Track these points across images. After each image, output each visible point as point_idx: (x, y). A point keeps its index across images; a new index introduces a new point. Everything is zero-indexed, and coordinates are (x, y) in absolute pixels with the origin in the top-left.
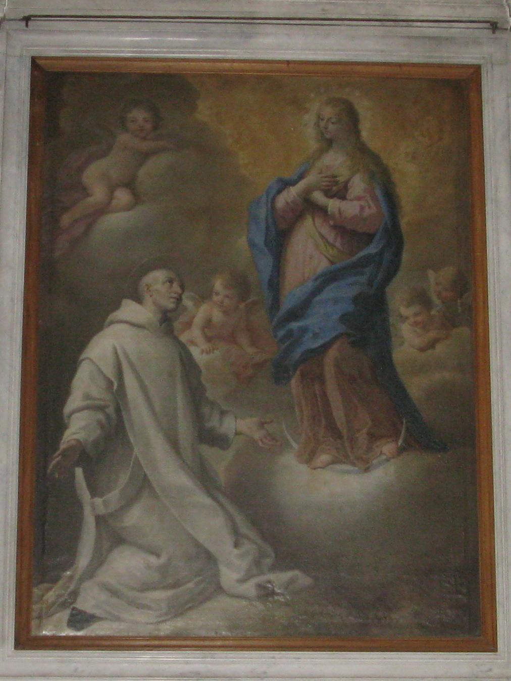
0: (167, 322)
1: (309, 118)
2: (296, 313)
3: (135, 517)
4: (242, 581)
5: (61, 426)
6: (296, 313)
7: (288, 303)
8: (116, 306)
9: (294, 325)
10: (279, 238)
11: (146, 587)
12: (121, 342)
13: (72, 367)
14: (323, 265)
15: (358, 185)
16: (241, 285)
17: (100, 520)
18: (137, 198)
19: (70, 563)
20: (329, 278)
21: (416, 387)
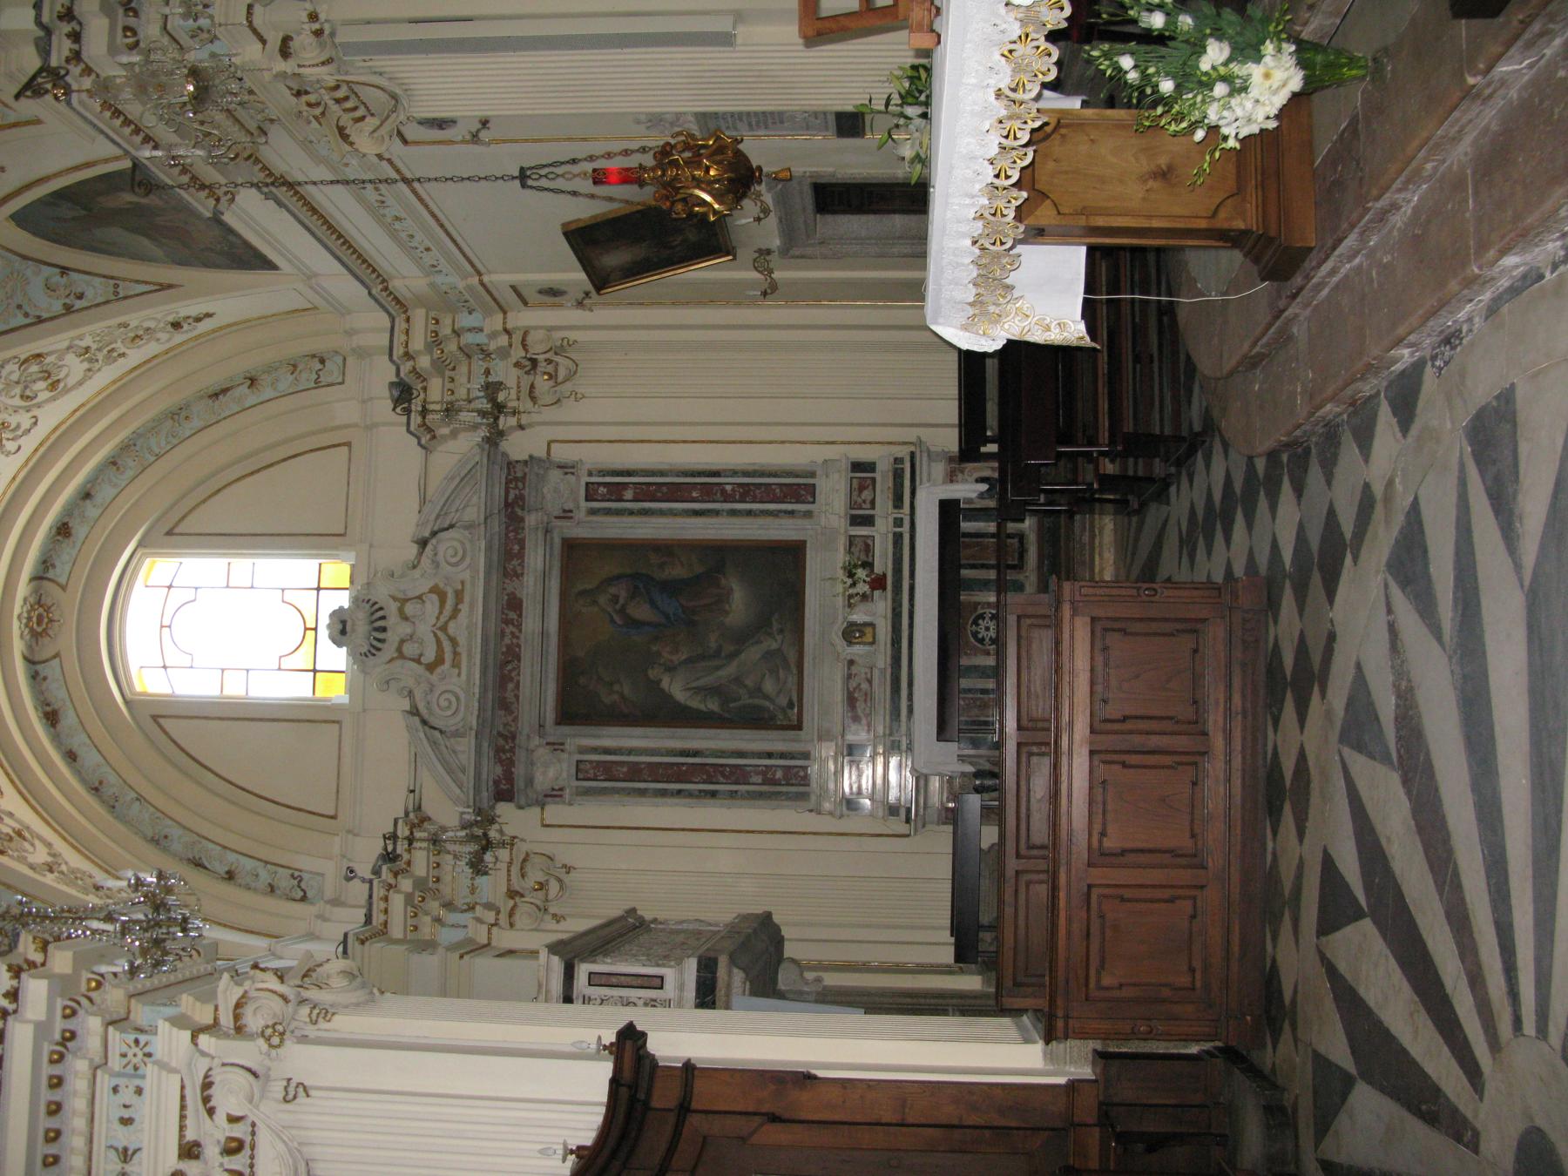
0: (671, 669)
1: (584, 610)
2: (667, 617)
3: (749, 682)
5: (712, 712)
6: (667, 617)
7: (663, 621)
8: (662, 690)
10: (635, 624)
12: (677, 689)
15: (613, 590)
20: (652, 603)
21: (699, 569)
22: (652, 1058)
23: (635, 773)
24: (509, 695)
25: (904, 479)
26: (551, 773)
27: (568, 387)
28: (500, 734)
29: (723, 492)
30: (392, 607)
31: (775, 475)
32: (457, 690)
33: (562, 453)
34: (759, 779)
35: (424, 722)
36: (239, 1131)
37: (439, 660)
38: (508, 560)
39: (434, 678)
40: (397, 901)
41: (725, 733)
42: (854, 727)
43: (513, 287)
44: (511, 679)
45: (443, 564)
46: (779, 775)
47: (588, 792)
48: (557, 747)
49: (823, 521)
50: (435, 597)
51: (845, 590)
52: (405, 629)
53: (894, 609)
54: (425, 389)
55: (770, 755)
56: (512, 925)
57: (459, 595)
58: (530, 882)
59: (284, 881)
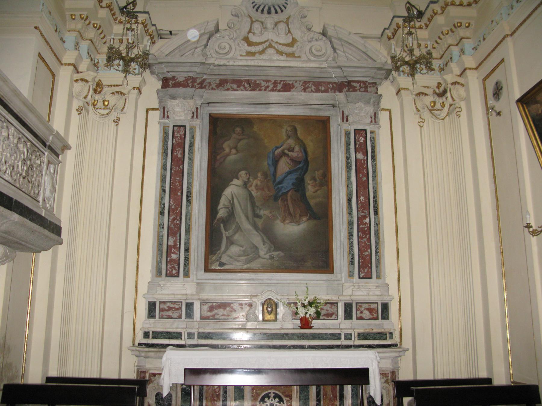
0: (246, 185)
1: (284, 130)
2: (280, 182)
3: (236, 237)
4: (265, 254)
5: (217, 213)
6: (280, 182)
7: (278, 180)
8: (232, 180)
9: (280, 186)
10: (275, 163)
11: (240, 256)
12: (233, 190)
13: (220, 197)
14: (288, 170)
15: (297, 148)
16: (265, 175)
17: (227, 238)
18: (238, 152)
19: (219, 249)
20: (289, 173)
21: (312, 202)
24: (229, 85)
25: (379, 340)
27: (426, 115)
28: (204, 81)
29: (365, 217)
30: (282, 16)
31: (377, 249)
32: (231, 55)
33: (383, 117)
37: (250, 44)
38: (316, 84)
41: (203, 221)
42: (206, 307)
43: (503, 60)
44: (238, 87)
45: (311, 44)
46: (174, 256)
48: (195, 114)
49: (347, 285)
50: (290, 40)
51: (300, 300)
52: (270, 23)
53: (287, 334)
54: (421, 28)
55: (187, 250)
56: (76, 81)
57: (291, 55)
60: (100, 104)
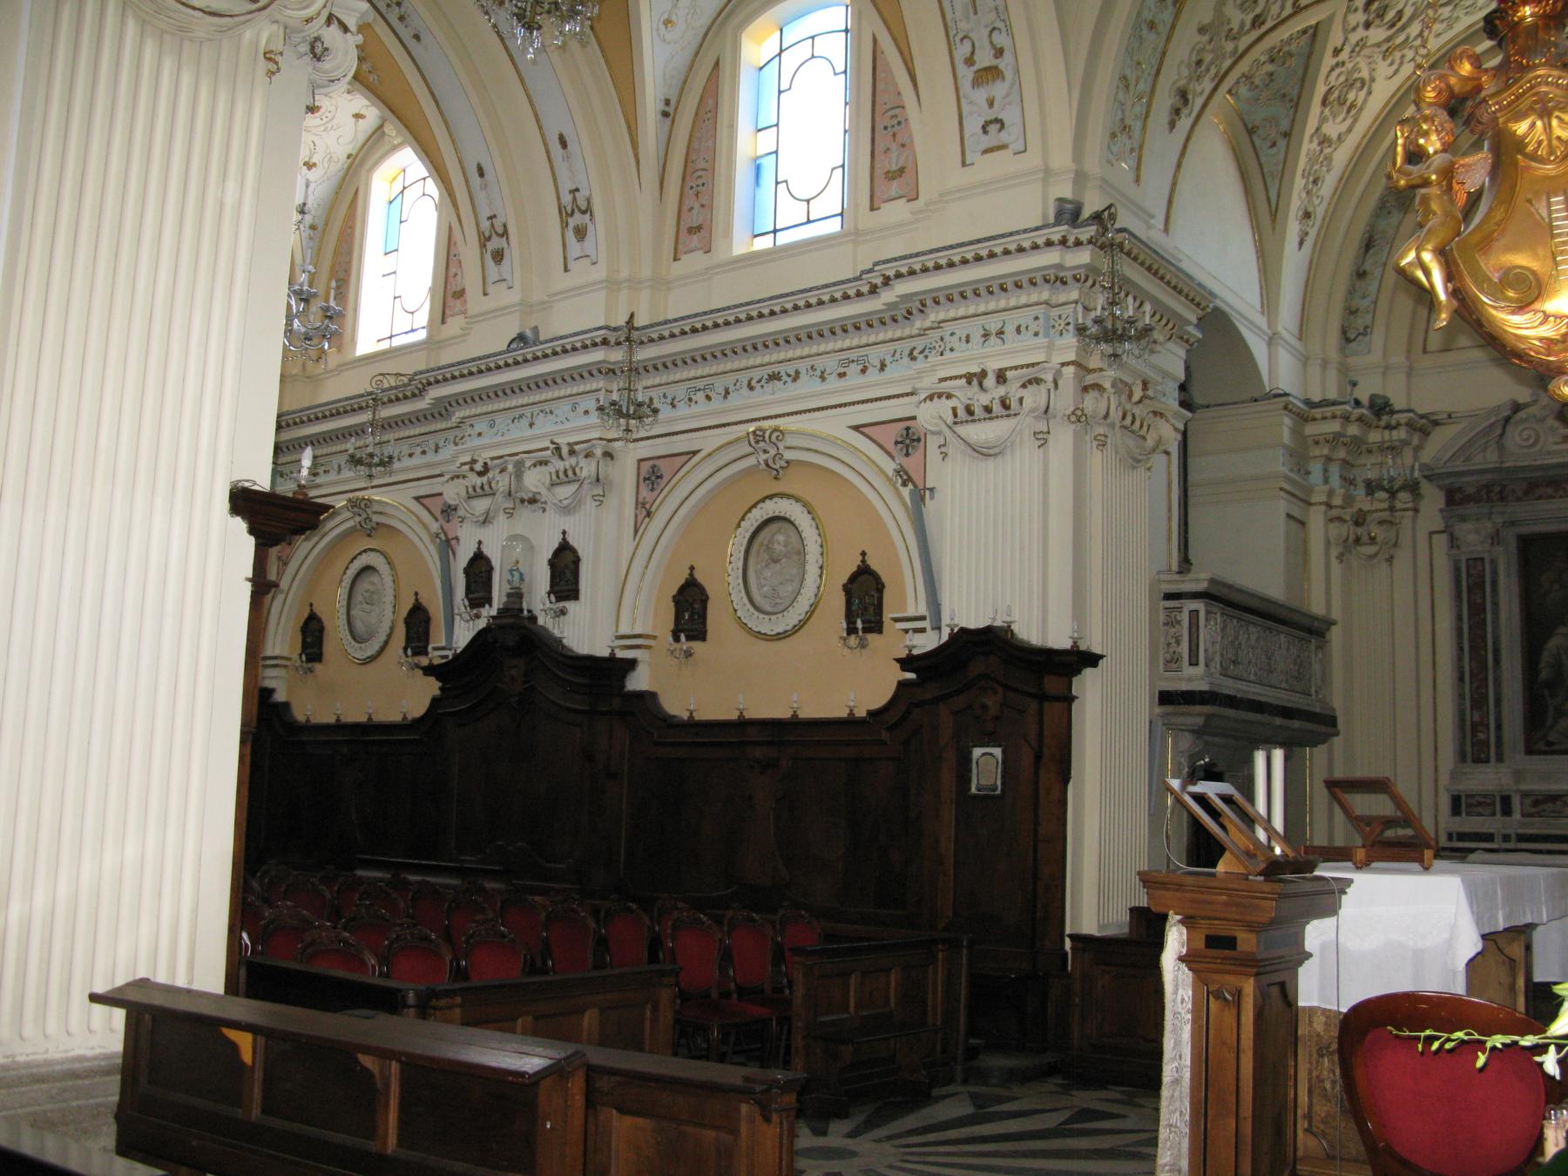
22: (1079, 672)
23: (1477, 610)
26: (1471, 537)
34: (1476, 718)
35: (1507, 420)
36: (1014, 405)
39: (1551, 422)
40: (1335, 426)
42: (1528, 801)
46: (1481, 736)
47: (1457, 570)
48: (1495, 538)
55: (1499, 727)
56: (1331, 520)
58: (1376, 530)
59: (1360, 322)
60: (1365, 539)
